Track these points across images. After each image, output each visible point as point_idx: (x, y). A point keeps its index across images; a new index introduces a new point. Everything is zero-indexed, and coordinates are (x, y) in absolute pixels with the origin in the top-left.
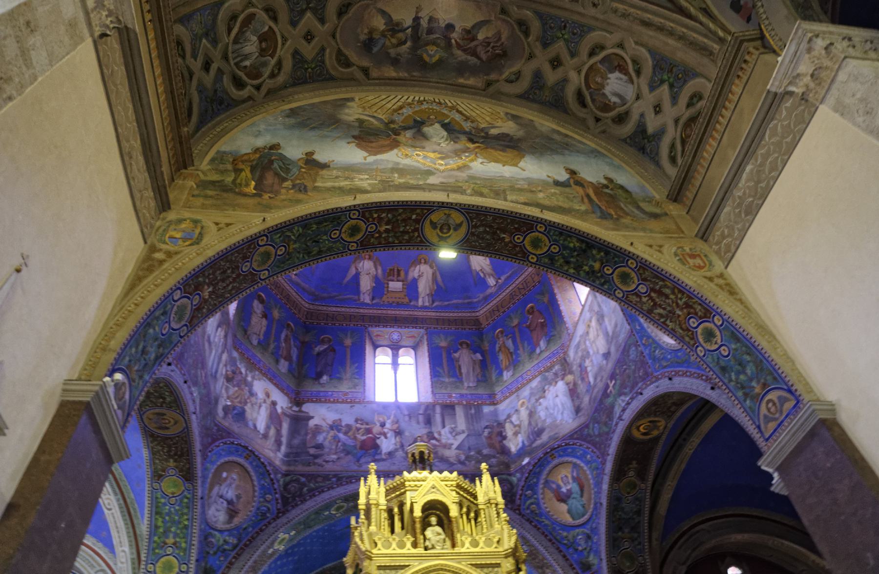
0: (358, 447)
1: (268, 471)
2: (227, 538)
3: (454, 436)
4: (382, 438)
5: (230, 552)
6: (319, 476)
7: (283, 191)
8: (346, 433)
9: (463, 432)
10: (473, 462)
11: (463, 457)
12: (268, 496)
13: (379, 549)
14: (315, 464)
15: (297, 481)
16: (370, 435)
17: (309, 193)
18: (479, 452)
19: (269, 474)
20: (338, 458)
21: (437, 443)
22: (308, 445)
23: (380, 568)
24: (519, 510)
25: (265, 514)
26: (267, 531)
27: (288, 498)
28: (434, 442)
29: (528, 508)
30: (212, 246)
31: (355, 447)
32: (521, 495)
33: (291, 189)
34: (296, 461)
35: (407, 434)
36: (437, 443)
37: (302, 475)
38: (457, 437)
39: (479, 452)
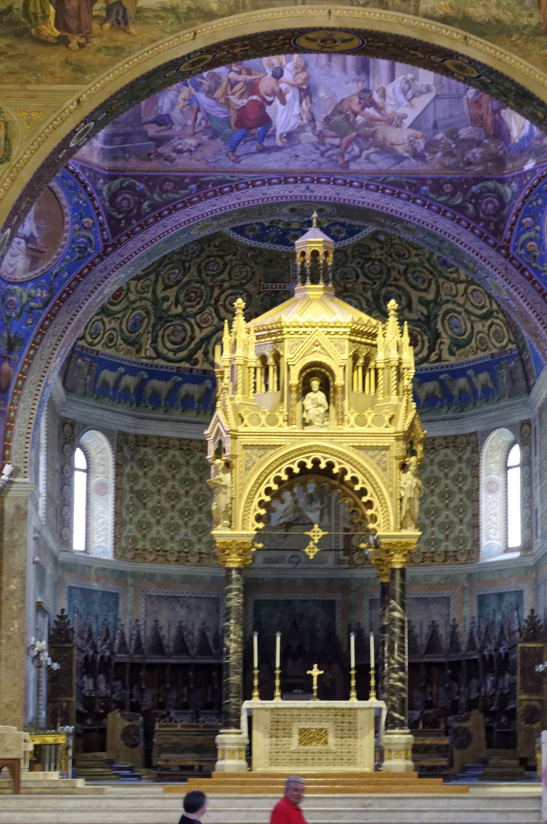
0: (233, 122)
1: (82, 183)
2: (33, 291)
3: (409, 100)
4: (277, 102)
5: (40, 311)
6: (167, 180)
7: (95, 26)
8: (210, 93)
9: (428, 89)
10: (439, 154)
11: (421, 144)
12: (85, 220)
13: (246, 426)
14: (159, 156)
15: (131, 188)
16: (255, 97)
17: (132, 29)
18: (453, 134)
19: (85, 187)
20: (199, 145)
21: (376, 114)
22: (145, 119)
23: (245, 447)
24: (507, 249)
25: (85, 248)
26: (91, 277)
27: (120, 221)
28: (370, 111)
29: (523, 246)
30: (26, 164)
31: (227, 121)
32: (513, 225)
33: (106, 20)
34: (124, 150)
35: (322, 94)
36: (376, 114)
37: (139, 178)
38: (415, 101)
39: (453, 134)
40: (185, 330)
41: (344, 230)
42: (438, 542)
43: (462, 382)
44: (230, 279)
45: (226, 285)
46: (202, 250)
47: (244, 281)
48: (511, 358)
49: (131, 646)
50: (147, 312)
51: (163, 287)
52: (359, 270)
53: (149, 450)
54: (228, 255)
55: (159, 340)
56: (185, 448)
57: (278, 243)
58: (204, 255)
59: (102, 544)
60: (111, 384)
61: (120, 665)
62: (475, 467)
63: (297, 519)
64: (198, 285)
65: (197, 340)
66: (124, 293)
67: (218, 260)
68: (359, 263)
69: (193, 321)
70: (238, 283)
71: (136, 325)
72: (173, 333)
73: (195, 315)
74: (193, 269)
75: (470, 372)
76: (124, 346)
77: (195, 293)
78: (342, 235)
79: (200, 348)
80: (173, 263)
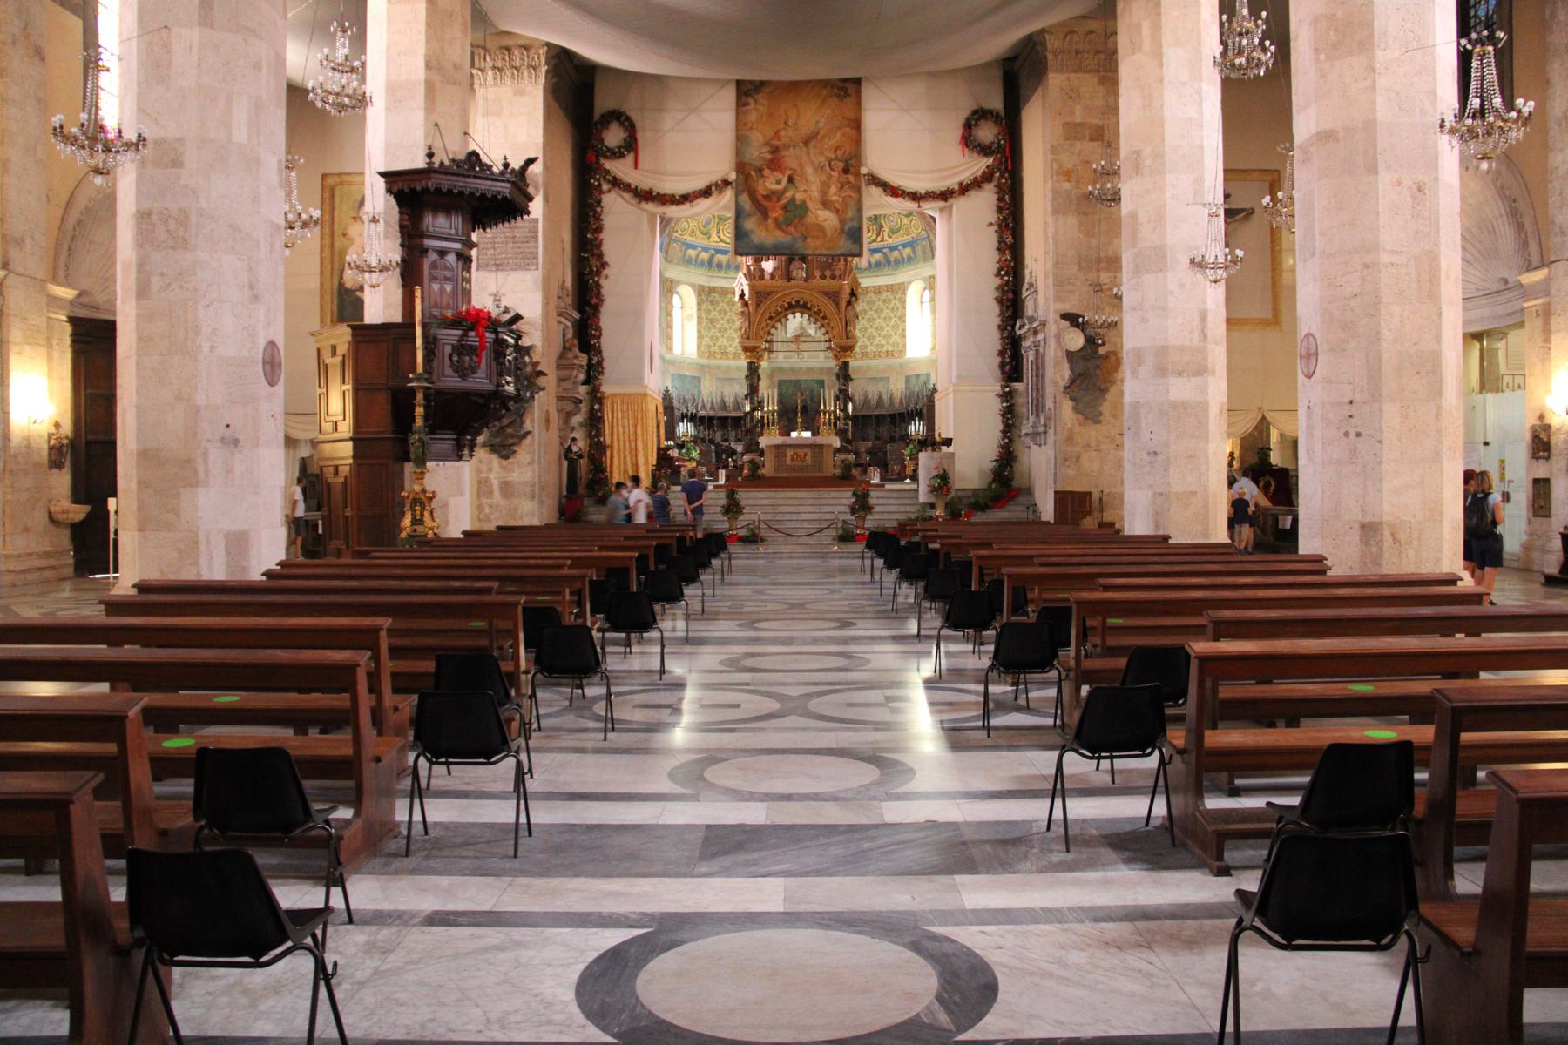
42: (883, 346)
43: (896, 253)
48: (924, 239)
49: (708, 406)
61: (702, 418)
62: (903, 302)
71: (708, 223)
75: (900, 247)
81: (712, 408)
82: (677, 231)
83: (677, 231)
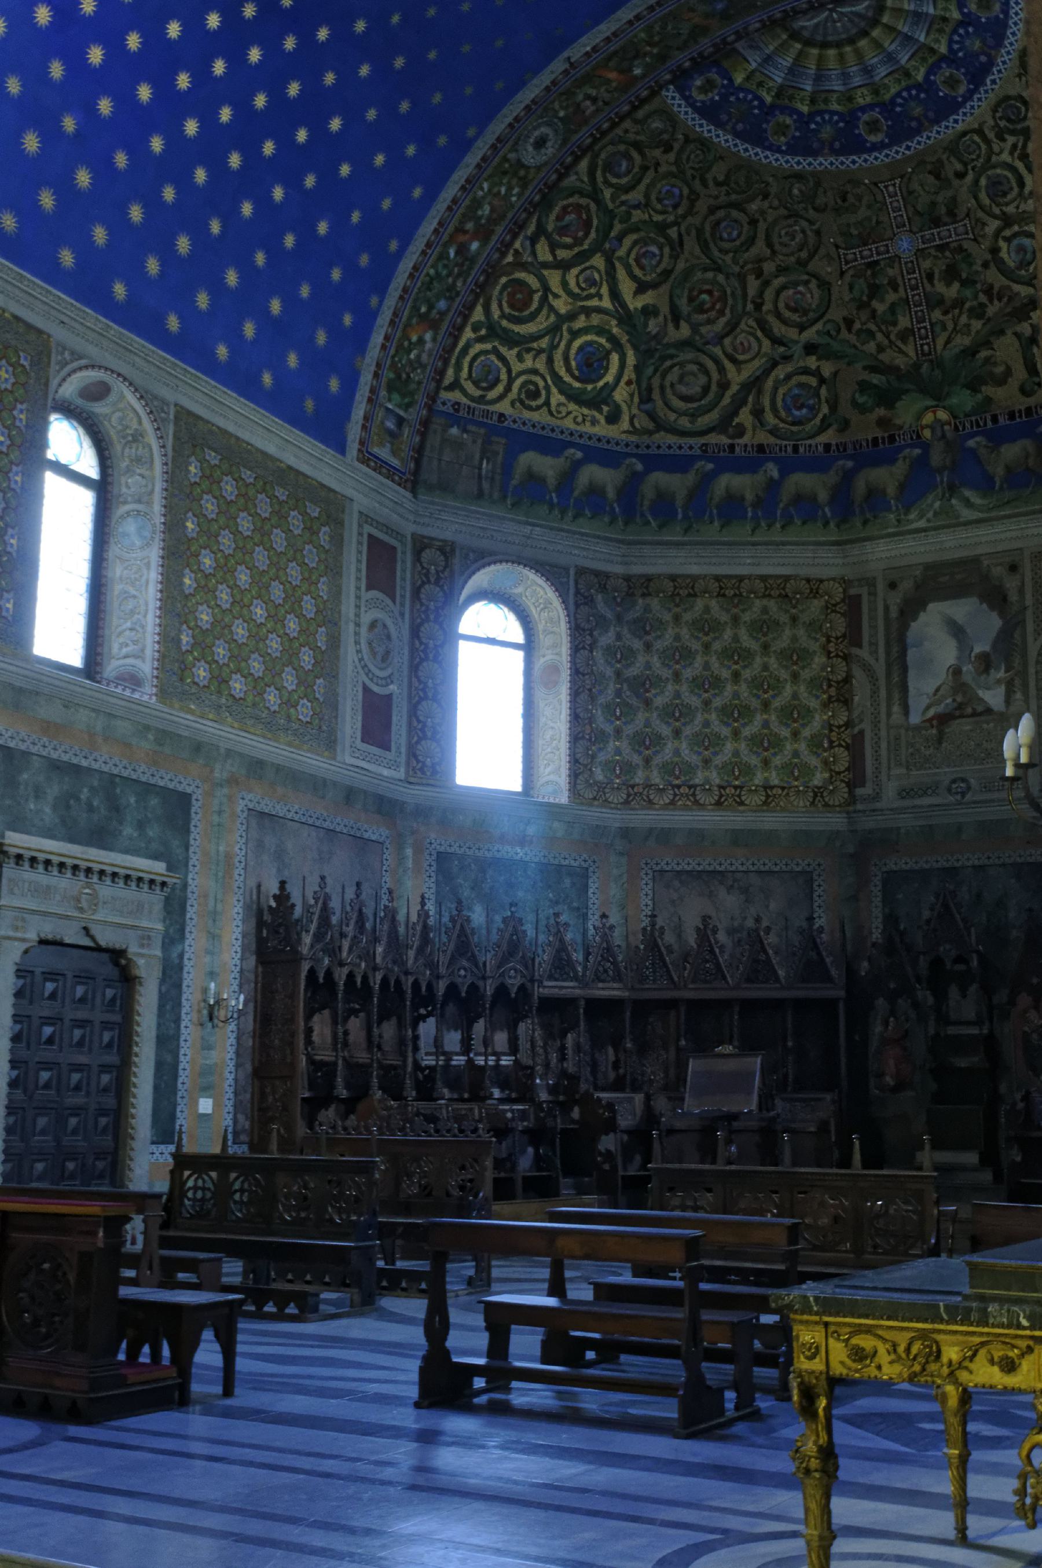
40: (707, 372)
41: (960, 74)
44: (774, 252)
45: (769, 267)
46: (694, 198)
47: (804, 255)
50: (612, 339)
51: (634, 286)
52: (1020, 166)
53: (655, 603)
54: (751, 199)
55: (656, 395)
56: (730, 593)
57: (845, 151)
58: (702, 206)
59: (552, 777)
60: (552, 481)
63: (960, 706)
64: (710, 275)
65: (734, 388)
66: (536, 297)
67: (735, 214)
68: (1014, 147)
69: (717, 351)
70: (793, 259)
72: (681, 379)
73: (720, 339)
74: (691, 244)
76: (572, 406)
77: (710, 293)
78: (962, 89)
79: (744, 402)
80: (637, 230)
81: (562, 965)
82: (455, 385)
83: (455, 385)
